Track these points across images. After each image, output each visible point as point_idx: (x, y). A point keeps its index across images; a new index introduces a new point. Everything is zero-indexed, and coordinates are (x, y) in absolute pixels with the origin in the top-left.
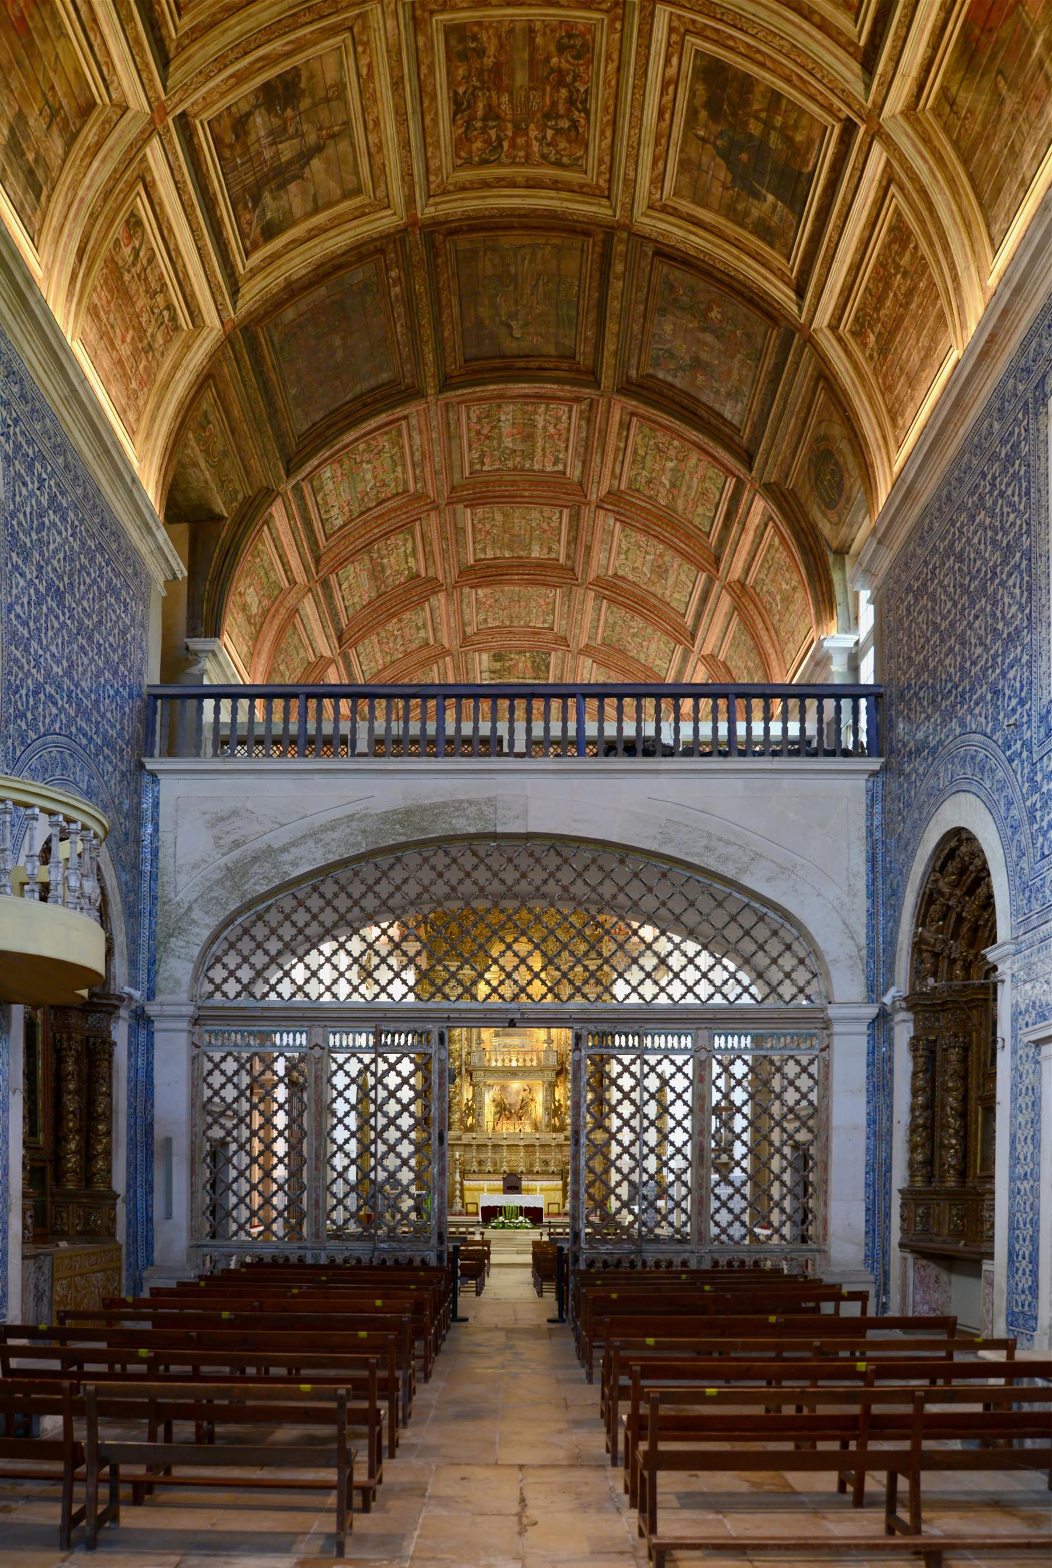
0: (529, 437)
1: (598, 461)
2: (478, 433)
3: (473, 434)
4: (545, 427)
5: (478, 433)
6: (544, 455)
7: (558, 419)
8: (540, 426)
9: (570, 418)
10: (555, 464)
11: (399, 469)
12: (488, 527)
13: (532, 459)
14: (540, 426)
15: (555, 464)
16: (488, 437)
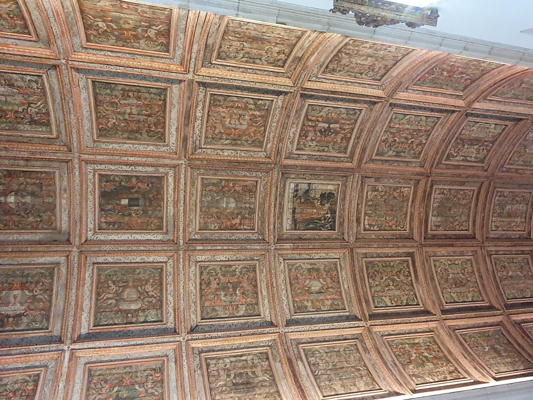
0: (509, 215)
1: (507, 244)
2: (517, 196)
3: (517, 194)
4: (514, 221)
5: (517, 196)
6: (500, 221)
7: (518, 226)
8: (515, 220)
9: (519, 231)
10: (496, 226)
11: (522, 163)
12: (459, 196)
13: (498, 217)
14: (515, 220)
15: (496, 226)
16: (513, 199)
